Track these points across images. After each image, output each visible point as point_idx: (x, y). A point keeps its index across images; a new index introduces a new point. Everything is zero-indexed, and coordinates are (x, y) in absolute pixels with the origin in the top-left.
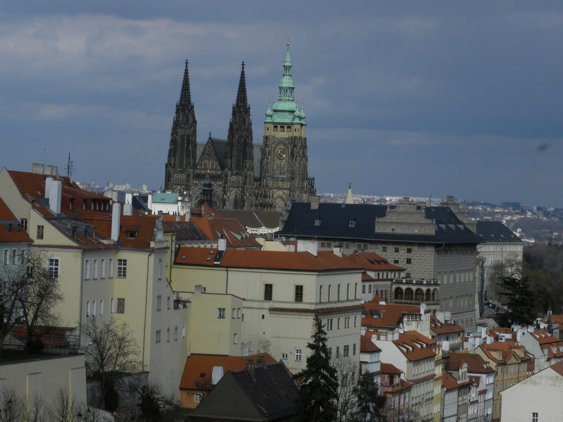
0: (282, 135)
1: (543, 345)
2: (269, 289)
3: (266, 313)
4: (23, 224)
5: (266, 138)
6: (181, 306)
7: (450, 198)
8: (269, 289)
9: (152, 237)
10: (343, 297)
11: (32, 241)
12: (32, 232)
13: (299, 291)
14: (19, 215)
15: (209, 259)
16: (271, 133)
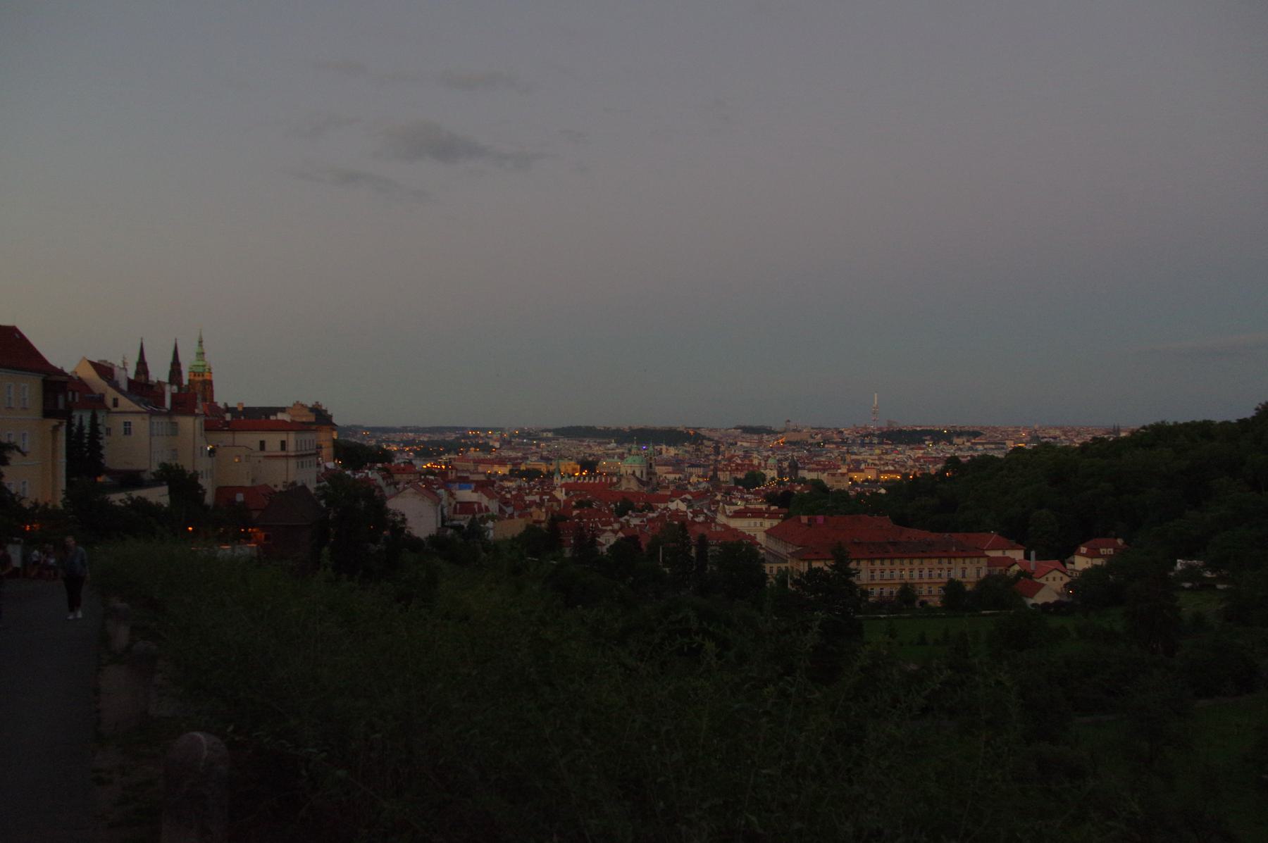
0: (197, 379)
1: (384, 479)
2: (262, 444)
3: (261, 459)
4: (101, 398)
5: (190, 380)
6: (212, 455)
7: (317, 403)
8: (262, 444)
9: (195, 406)
10: (308, 447)
11: (109, 409)
12: (109, 402)
13: (283, 445)
14: (97, 391)
15: (220, 426)
16: (192, 378)
